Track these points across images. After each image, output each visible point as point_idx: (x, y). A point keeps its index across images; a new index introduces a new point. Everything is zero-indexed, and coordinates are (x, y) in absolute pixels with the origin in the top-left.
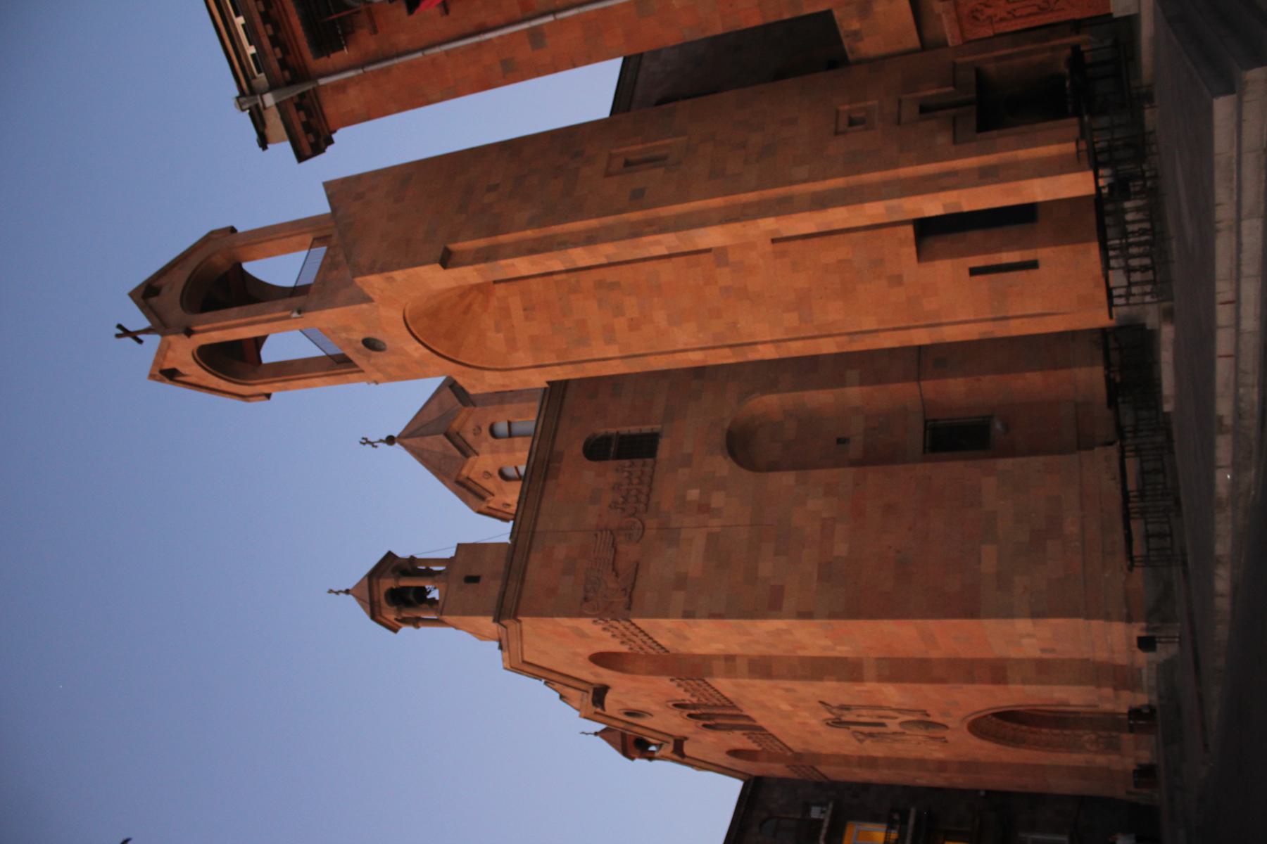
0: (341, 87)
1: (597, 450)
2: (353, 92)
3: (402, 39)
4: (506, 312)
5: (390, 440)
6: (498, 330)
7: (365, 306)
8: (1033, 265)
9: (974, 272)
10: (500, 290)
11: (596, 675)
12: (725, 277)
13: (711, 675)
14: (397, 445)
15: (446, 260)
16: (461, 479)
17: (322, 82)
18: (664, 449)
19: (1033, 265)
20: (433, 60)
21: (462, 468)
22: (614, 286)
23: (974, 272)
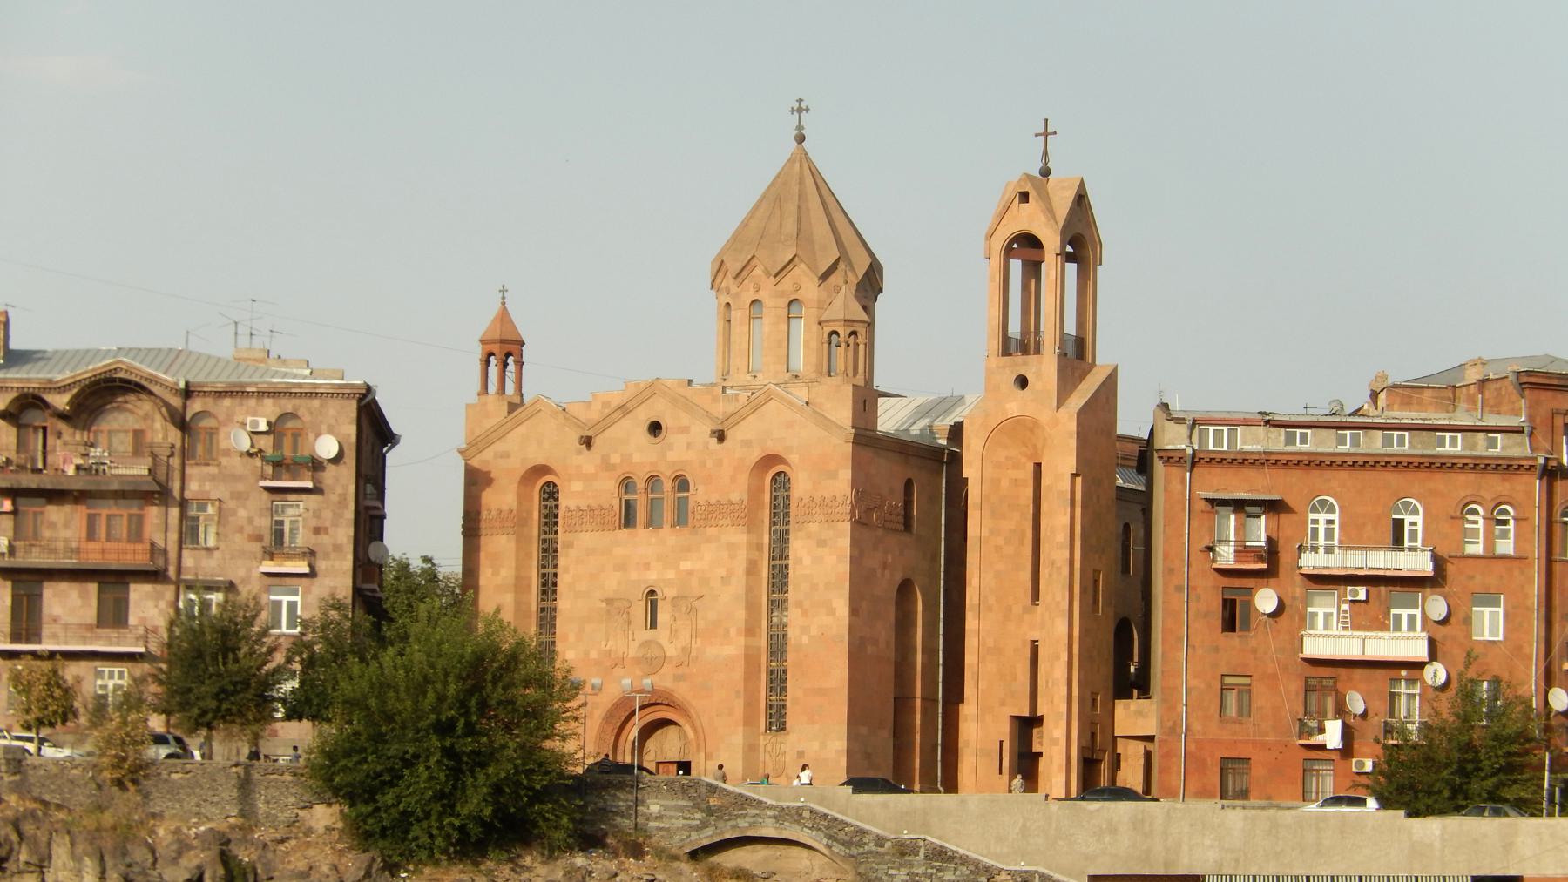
0: (1183, 481)
1: (909, 485)
2: (1179, 487)
3: (1195, 524)
4: (1016, 466)
5: (801, 139)
6: (1007, 458)
7: (1055, 404)
8: (1001, 773)
9: (1001, 742)
10: (1030, 467)
11: (747, 443)
12: (1017, 609)
13: (749, 532)
14: (795, 144)
15: (1074, 476)
16: (796, 259)
17: (1188, 474)
18: (905, 538)
19: (1001, 773)
20: (1182, 535)
21: (807, 266)
22: (1022, 543)
23: (1001, 742)
